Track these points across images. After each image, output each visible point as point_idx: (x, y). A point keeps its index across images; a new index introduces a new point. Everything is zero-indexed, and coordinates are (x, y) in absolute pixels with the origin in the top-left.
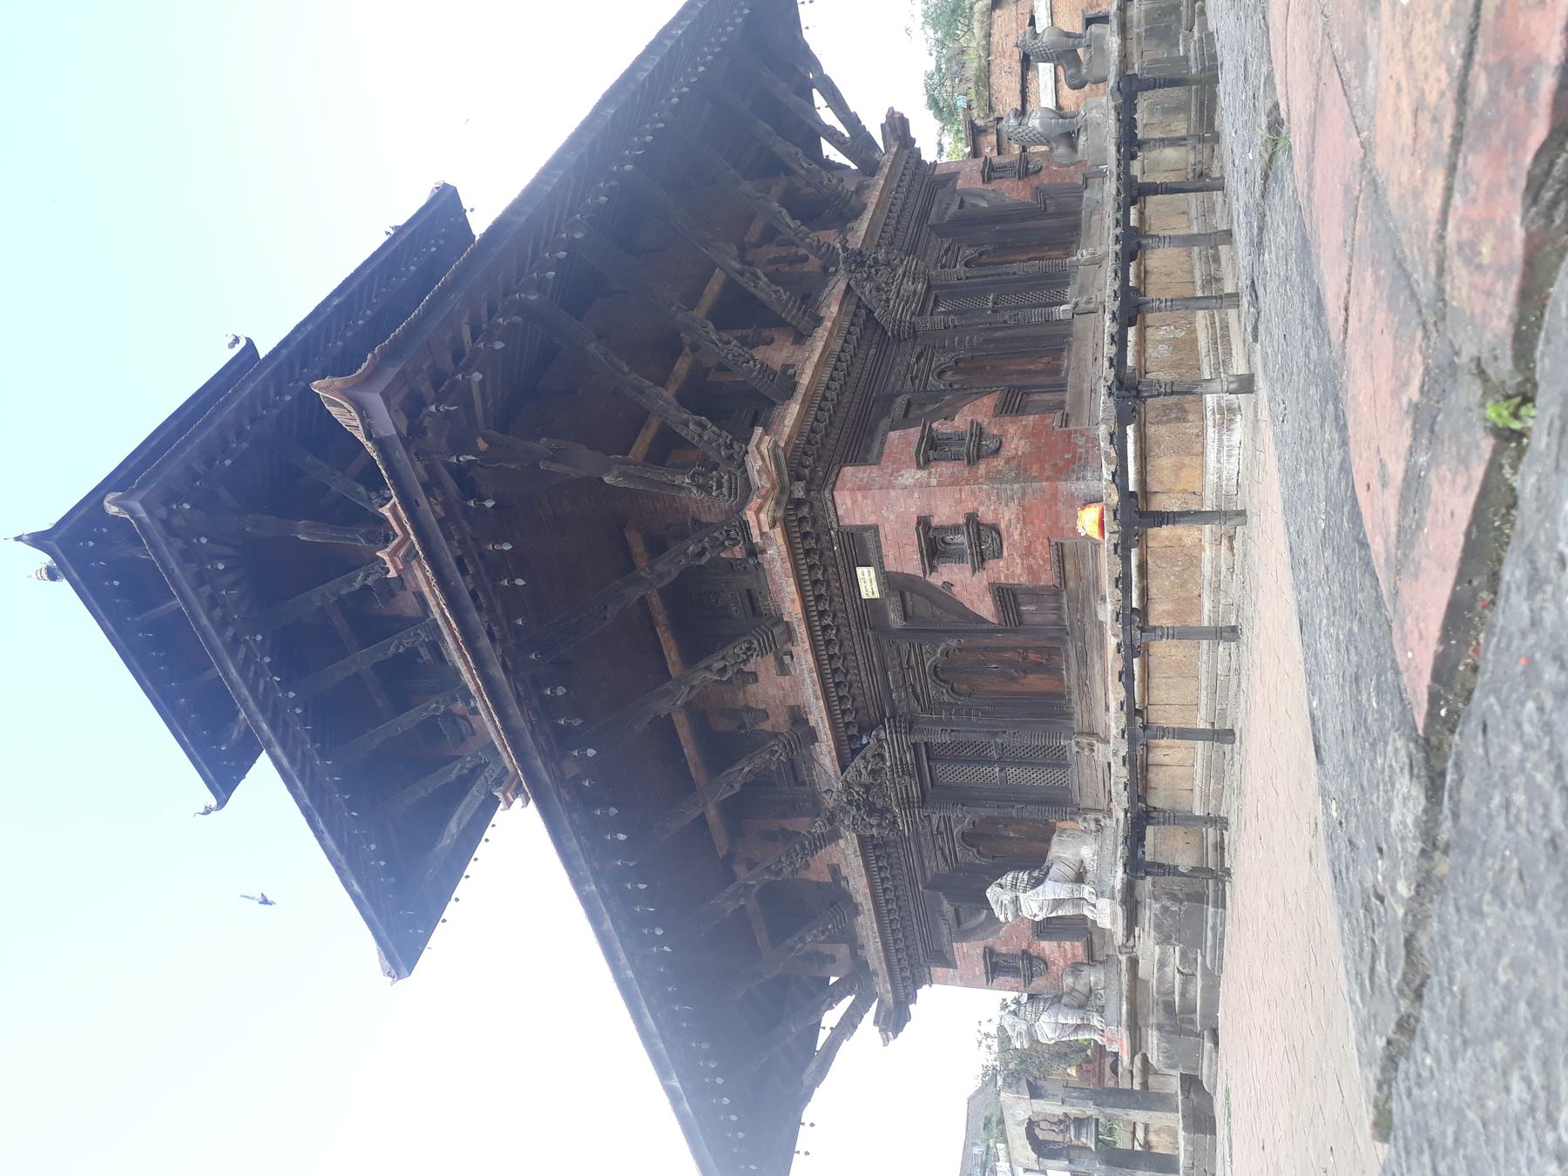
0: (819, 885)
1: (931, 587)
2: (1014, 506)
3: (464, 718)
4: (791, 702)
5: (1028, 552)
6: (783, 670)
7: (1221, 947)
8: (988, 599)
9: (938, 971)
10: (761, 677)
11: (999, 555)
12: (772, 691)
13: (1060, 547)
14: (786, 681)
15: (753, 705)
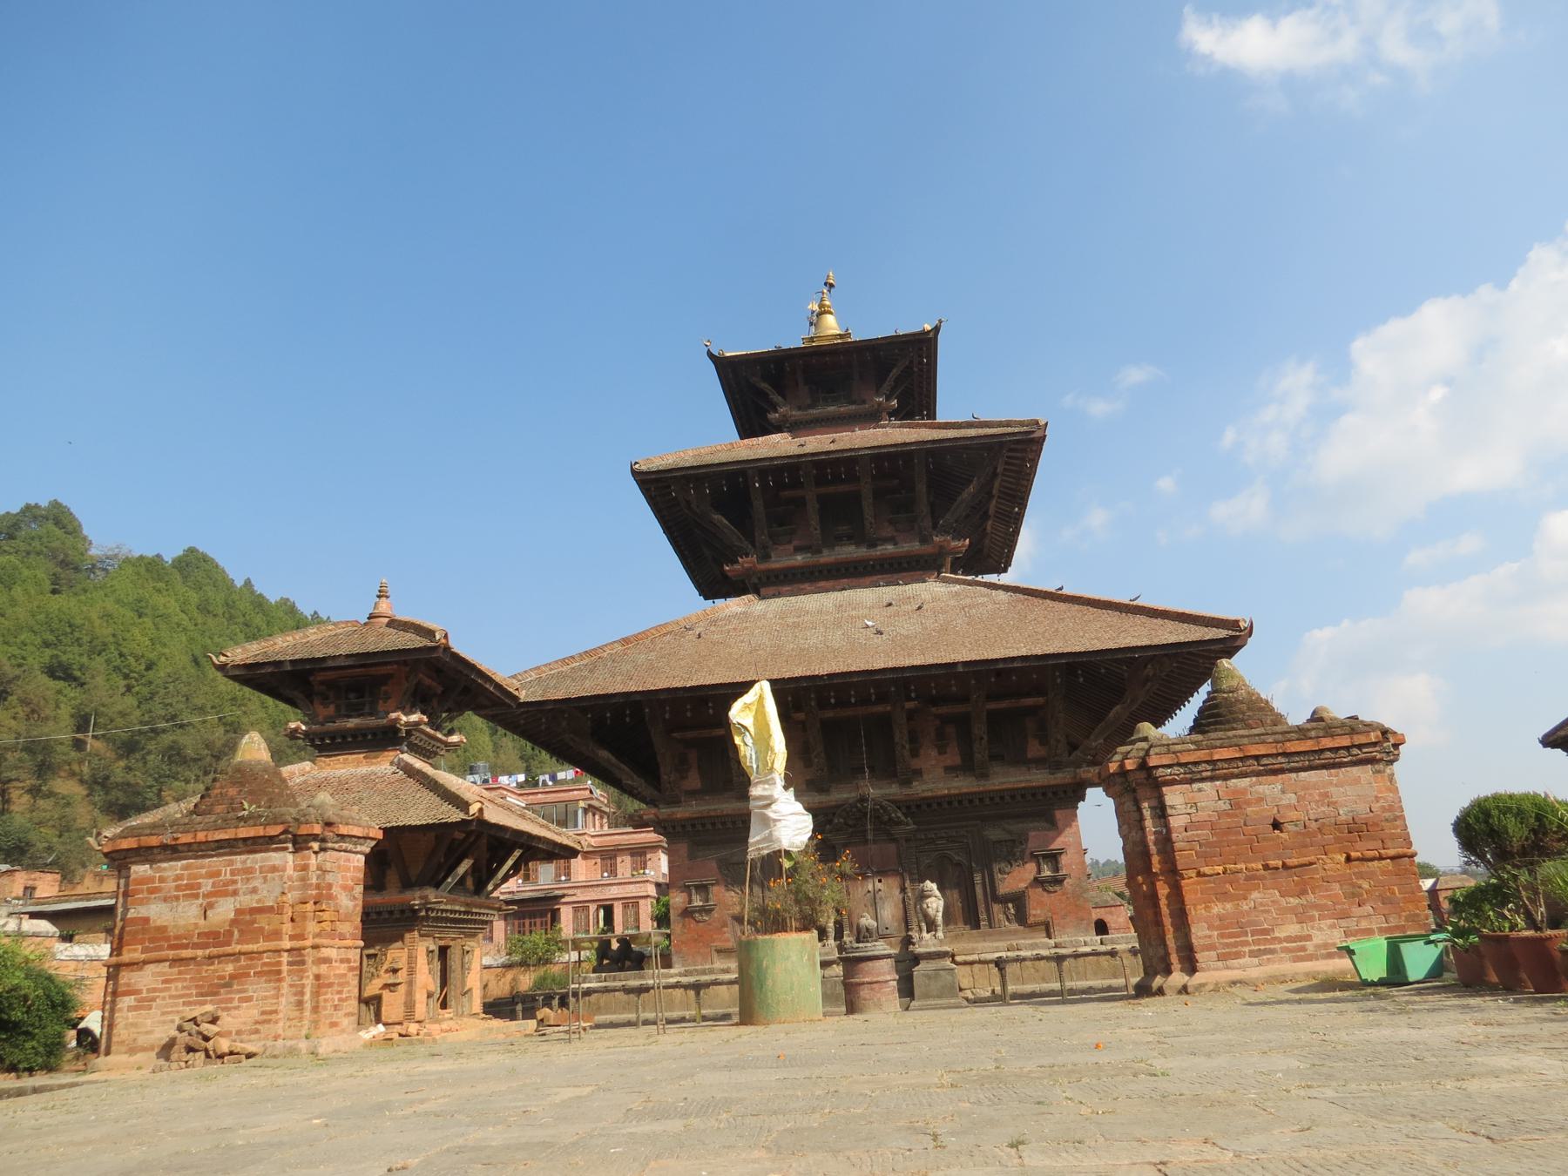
6: (948, 769)
9: (683, 848)
14: (940, 771)
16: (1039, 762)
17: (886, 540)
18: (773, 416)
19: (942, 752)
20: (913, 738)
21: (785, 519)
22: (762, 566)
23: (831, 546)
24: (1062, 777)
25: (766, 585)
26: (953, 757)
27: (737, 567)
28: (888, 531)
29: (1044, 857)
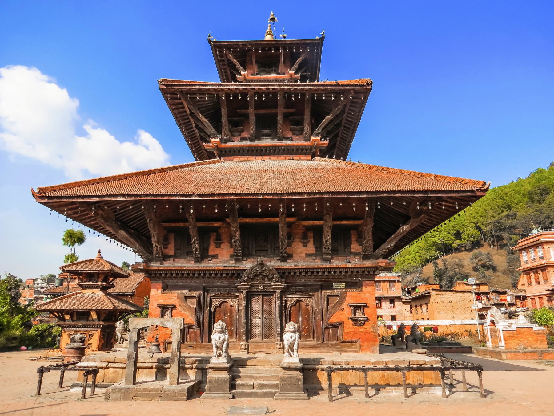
0: (207, 250)
1: (342, 304)
2: (371, 330)
3: (240, 135)
4: (294, 255)
5: (355, 333)
6: (308, 255)
7: (289, 399)
8: (337, 321)
9: (160, 285)
10: (305, 248)
11: (353, 325)
12: (299, 250)
13: (356, 342)
14: (303, 255)
15: (293, 243)
16: (356, 254)
17: (287, 138)
18: (238, 77)
19: (305, 245)
20: (290, 236)
21: (237, 124)
22: (223, 145)
23: (259, 139)
24: (368, 263)
25: (224, 155)
26: (311, 248)
27: (210, 145)
28: (290, 134)
29: (355, 307)
